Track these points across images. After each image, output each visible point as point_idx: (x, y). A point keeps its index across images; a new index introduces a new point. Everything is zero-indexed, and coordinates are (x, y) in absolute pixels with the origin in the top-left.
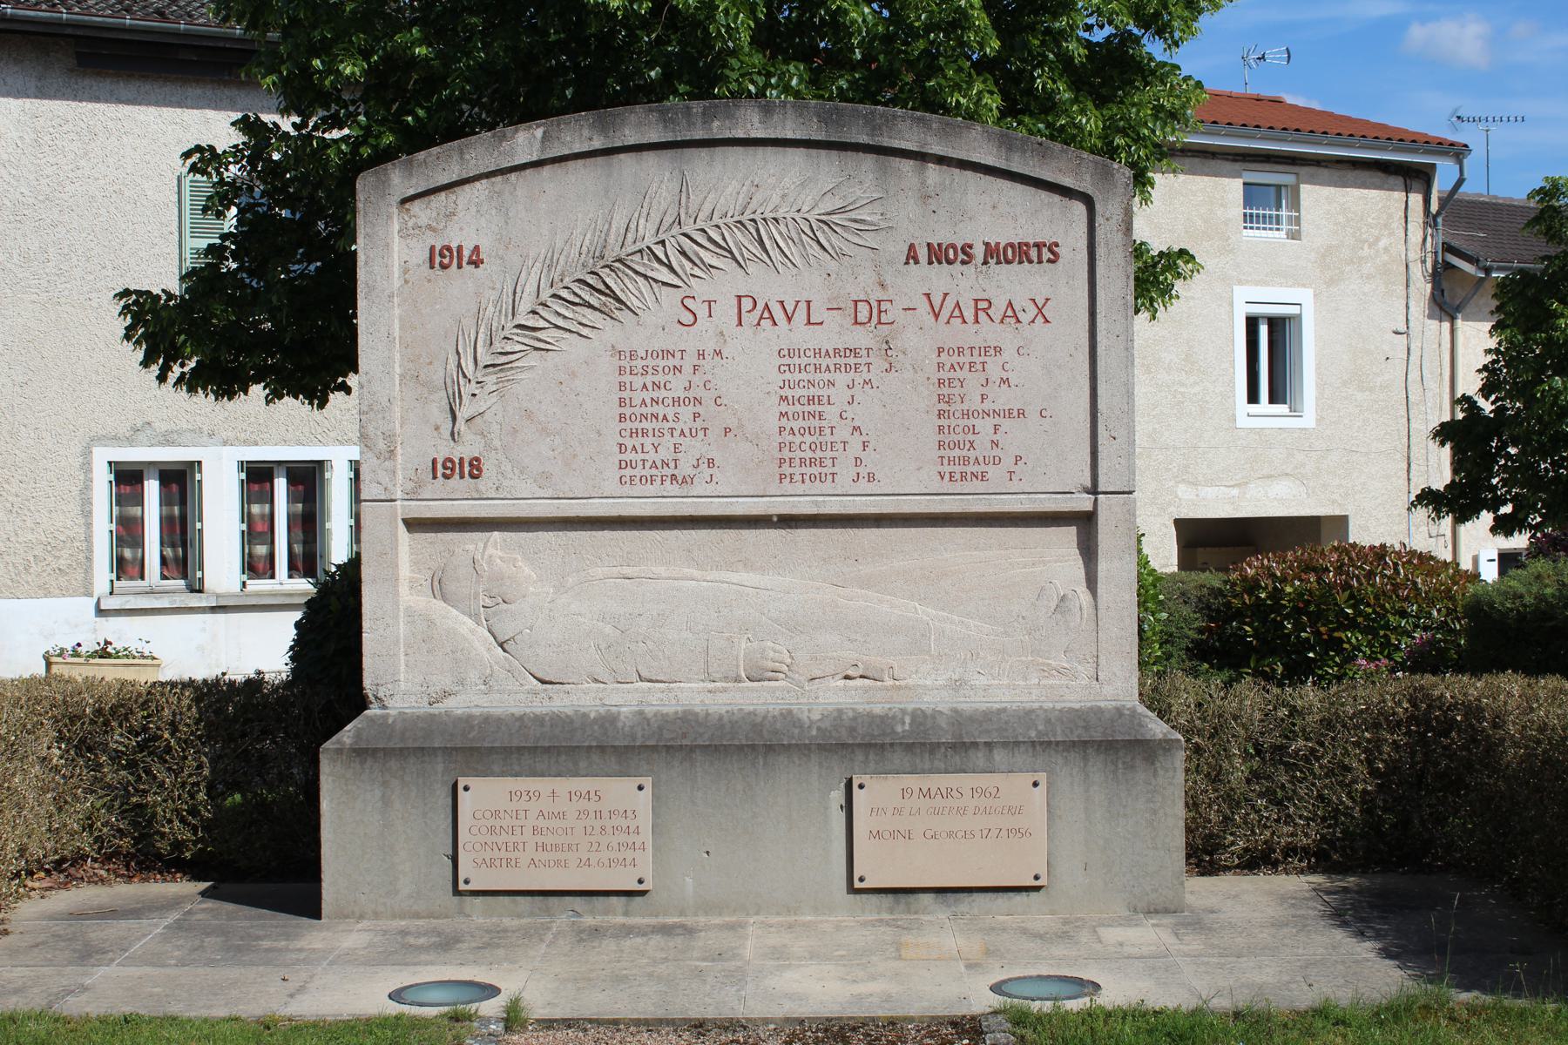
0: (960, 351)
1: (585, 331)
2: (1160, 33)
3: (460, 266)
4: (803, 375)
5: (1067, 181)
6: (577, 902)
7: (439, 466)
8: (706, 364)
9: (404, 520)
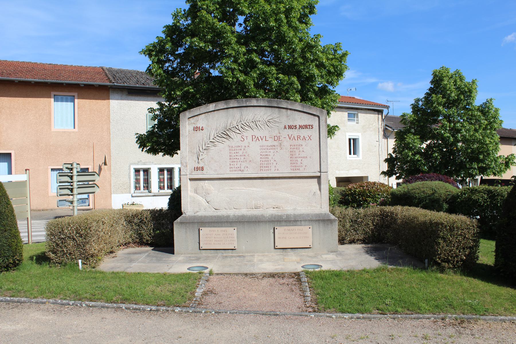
0: (295, 145)
2: (332, 85)
5: (315, 113)
6: (223, 251)
8: (246, 148)
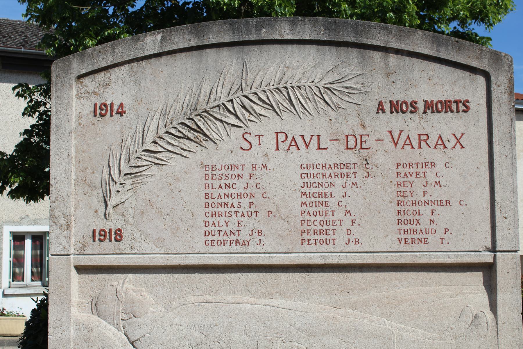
0: (410, 165)
1: (185, 153)
2: (483, 20)
3: (111, 115)
4: (316, 180)
5: (474, 64)
7: (113, 233)
8: (258, 173)
9: (74, 266)
